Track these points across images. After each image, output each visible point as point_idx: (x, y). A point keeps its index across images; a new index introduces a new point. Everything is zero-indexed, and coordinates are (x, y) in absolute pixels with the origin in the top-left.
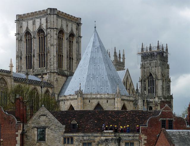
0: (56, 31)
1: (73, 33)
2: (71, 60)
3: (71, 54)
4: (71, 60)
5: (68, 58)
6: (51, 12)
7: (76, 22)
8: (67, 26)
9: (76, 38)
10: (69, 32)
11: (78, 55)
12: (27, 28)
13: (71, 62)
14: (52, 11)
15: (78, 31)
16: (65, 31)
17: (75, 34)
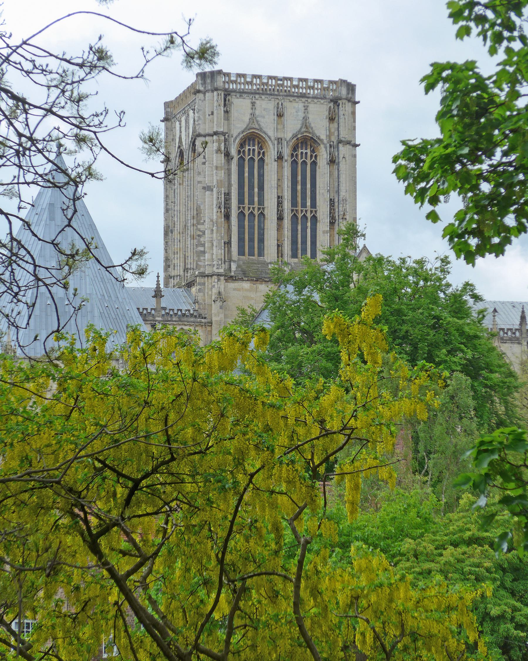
0: (219, 141)
1: (313, 133)
2: (309, 224)
3: (309, 204)
4: (309, 224)
5: (287, 223)
6: (204, 83)
7: (324, 98)
8: (280, 115)
9: (326, 148)
10: (289, 135)
11: (336, 204)
12: (180, 138)
13: (309, 231)
14: (208, 81)
15: (336, 125)
16: (271, 133)
17: (323, 137)
